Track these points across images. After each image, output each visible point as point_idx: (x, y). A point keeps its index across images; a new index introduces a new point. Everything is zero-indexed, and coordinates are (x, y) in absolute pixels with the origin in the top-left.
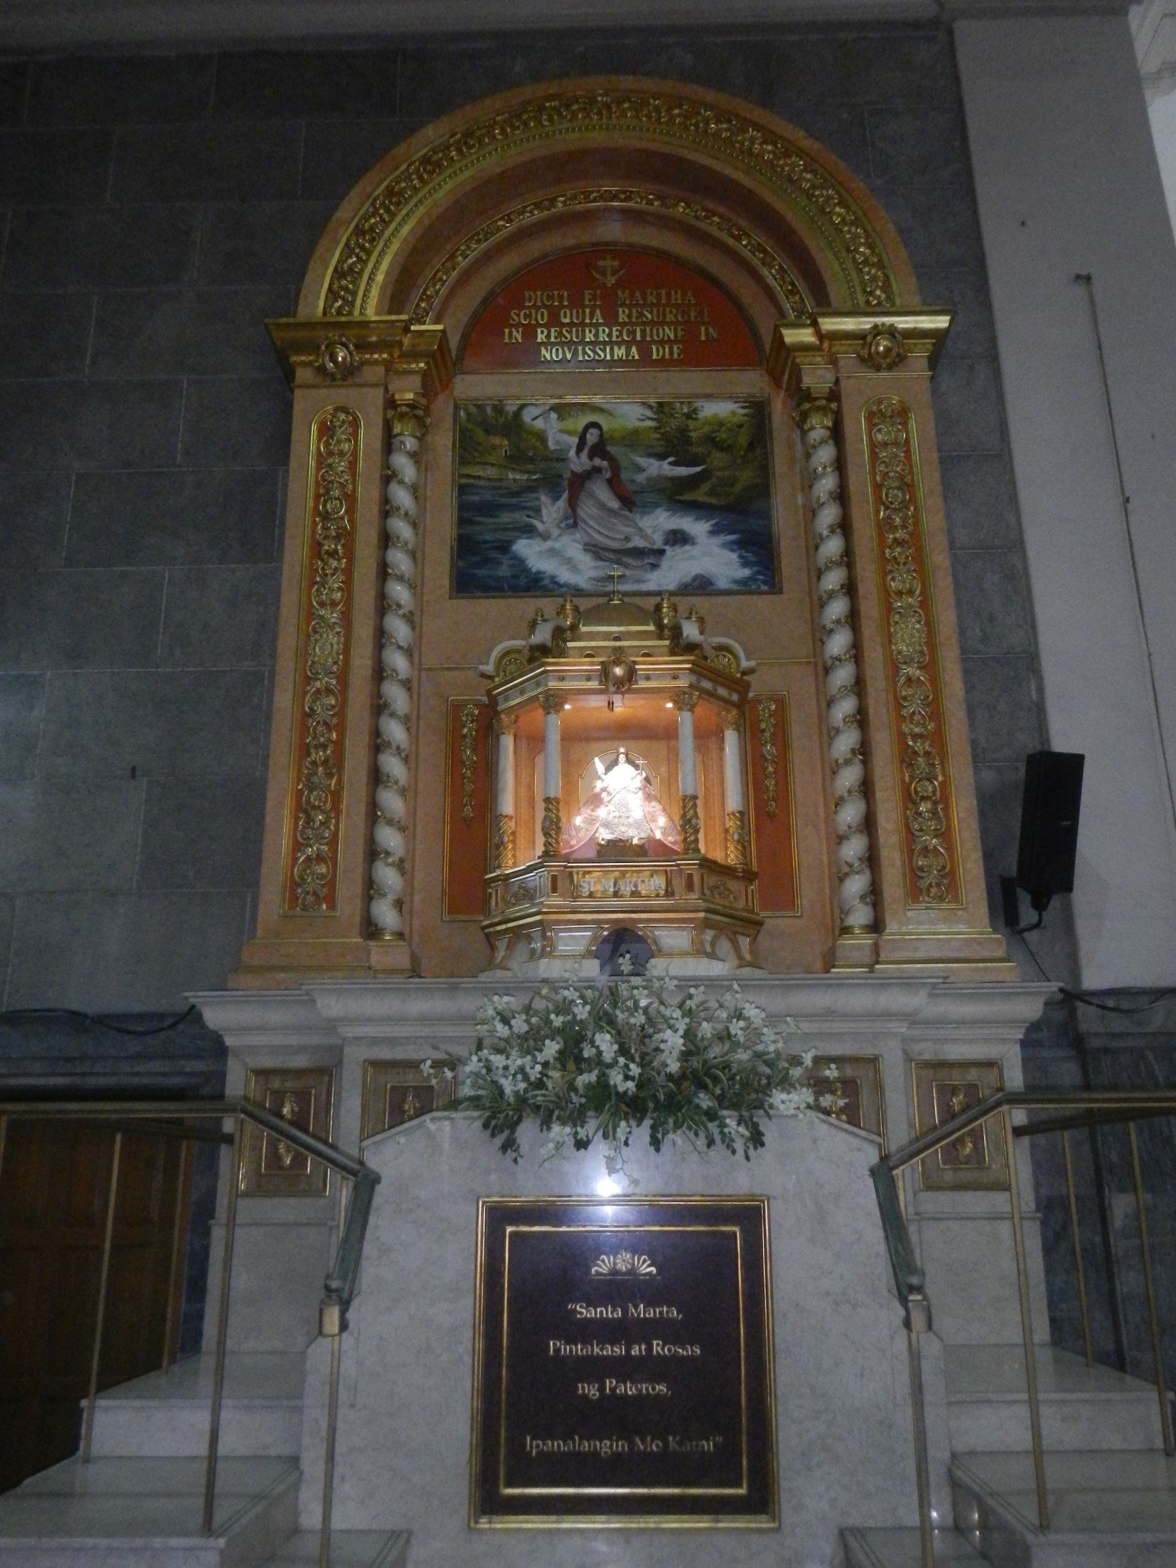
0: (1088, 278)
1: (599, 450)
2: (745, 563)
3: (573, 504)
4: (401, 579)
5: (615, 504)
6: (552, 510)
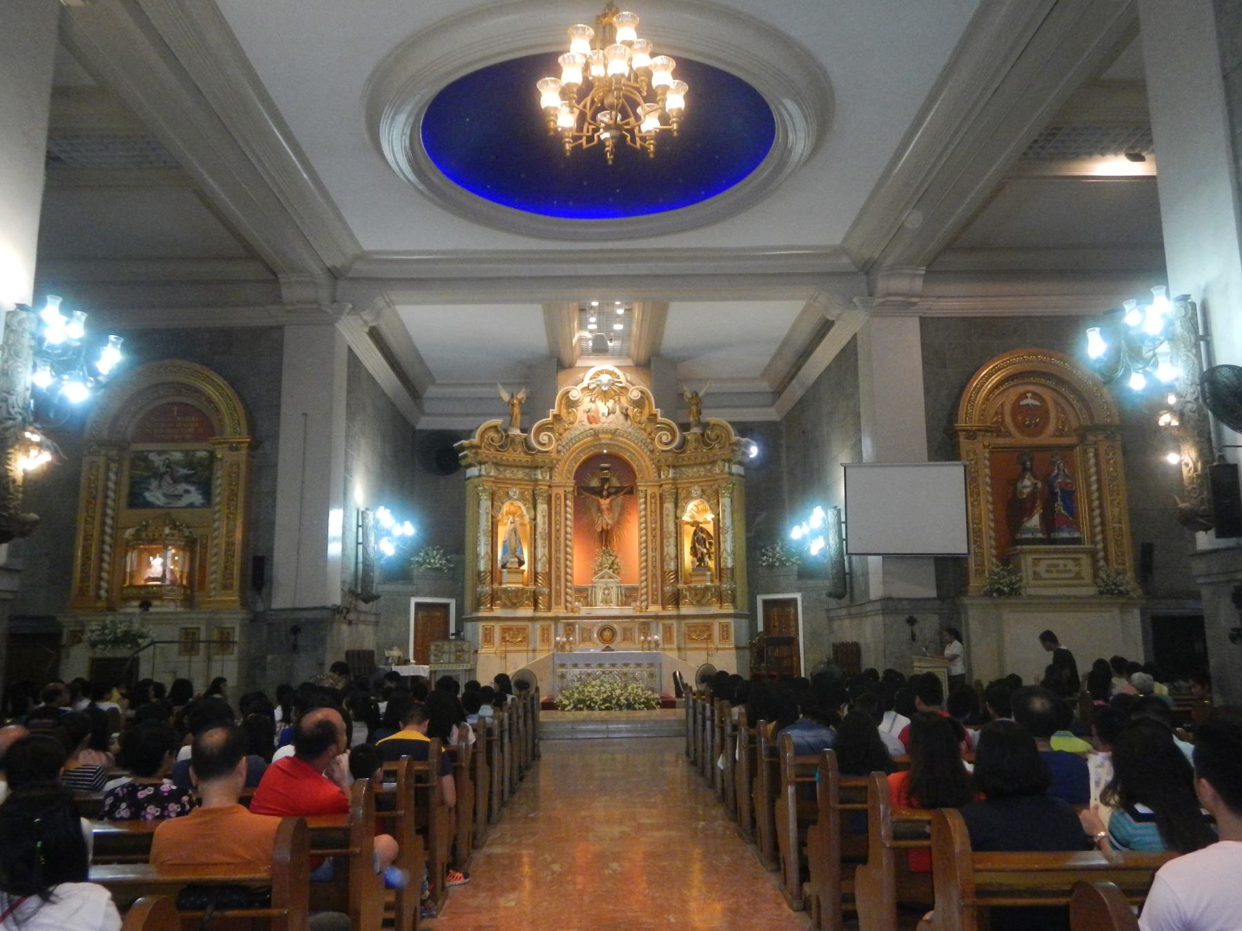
0: (305, 414)
1: (168, 466)
2: (204, 499)
3: (160, 482)
4: (110, 508)
5: (171, 482)
6: (154, 483)
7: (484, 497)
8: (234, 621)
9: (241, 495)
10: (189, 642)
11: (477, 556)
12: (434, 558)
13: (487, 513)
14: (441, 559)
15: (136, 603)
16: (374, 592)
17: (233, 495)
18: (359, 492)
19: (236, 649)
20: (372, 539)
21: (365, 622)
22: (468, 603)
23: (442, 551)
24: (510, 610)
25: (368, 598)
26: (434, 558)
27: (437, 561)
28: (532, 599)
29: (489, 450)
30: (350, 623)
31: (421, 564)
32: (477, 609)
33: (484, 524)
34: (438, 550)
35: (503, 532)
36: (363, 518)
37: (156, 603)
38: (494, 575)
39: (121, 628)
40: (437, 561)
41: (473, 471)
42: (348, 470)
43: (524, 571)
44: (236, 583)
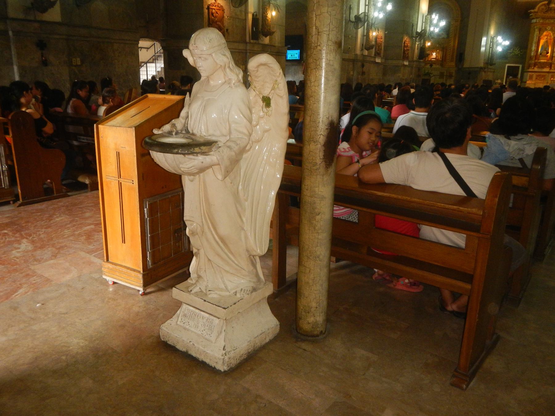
7: (537, 30)
8: (453, 71)
9: (457, 36)
10: (442, 75)
11: (531, 51)
12: (516, 51)
13: (537, 36)
14: (518, 51)
15: (429, 65)
16: (494, 63)
17: (455, 35)
18: (492, 32)
19: (453, 78)
20: (495, 46)
21: (490, 72)
22: (526, 65)
23: (519, 49)
24: (540, 69)
25: (491, 65)
26: (516, 51)
27: (517, 52)
28: (549, 65)
29: (541, 13)
30: (485, 72)
31: (511, 53)
32: (529, 69)
33: (535, 40)
34: (518, 48)
35: (542, 42)
36: (493, 40)
37: (434, 65)
38: (537, 57)
39: (427, 71)
40: (517, 52)
41: (534, 21)
42: (489, 26)
43: (548, 56)
44: (455, 60)
